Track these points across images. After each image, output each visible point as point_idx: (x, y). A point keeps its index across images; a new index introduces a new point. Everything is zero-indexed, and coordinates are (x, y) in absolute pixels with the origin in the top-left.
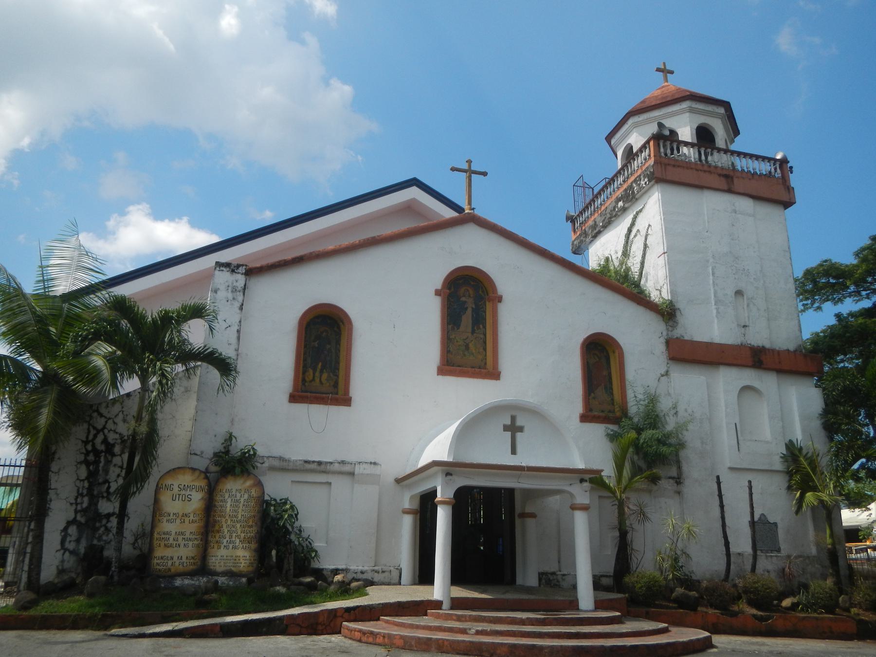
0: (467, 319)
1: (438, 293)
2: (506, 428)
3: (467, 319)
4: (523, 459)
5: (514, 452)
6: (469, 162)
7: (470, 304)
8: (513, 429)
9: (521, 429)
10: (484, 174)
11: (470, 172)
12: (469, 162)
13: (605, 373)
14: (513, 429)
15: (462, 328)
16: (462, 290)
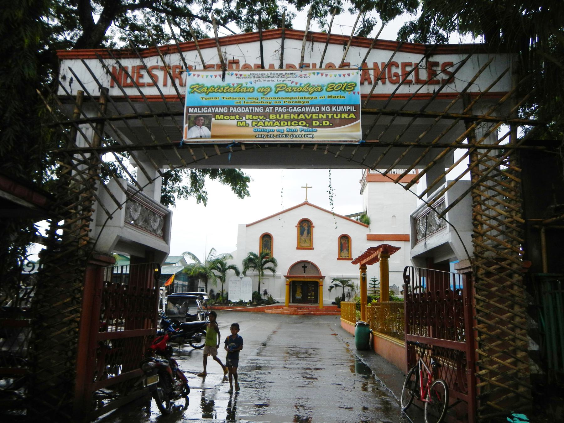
0: (305, 233)
1: (296, 227)
2: (303, 267)
3: (305, 233)
4: (305, 275)
5: (305, 272)
6: (307, 184)
7: (306, 228)
8: (305, 267)
9: (306, 267)
10: (311, 187)
11: (307, 187)
12: (307, 184)
13: (347, 245)
14: (305, 267)
15: (304, 235)
16: (304, 225)
